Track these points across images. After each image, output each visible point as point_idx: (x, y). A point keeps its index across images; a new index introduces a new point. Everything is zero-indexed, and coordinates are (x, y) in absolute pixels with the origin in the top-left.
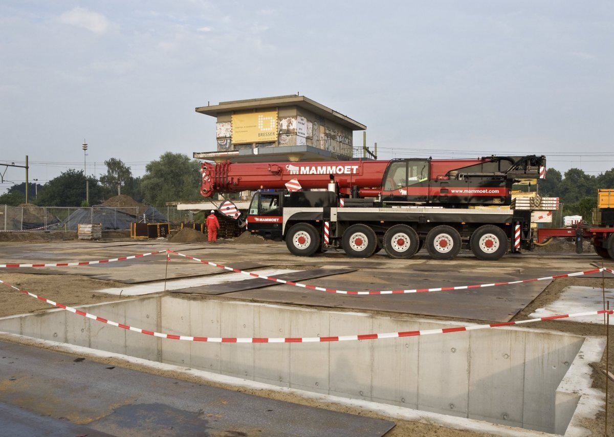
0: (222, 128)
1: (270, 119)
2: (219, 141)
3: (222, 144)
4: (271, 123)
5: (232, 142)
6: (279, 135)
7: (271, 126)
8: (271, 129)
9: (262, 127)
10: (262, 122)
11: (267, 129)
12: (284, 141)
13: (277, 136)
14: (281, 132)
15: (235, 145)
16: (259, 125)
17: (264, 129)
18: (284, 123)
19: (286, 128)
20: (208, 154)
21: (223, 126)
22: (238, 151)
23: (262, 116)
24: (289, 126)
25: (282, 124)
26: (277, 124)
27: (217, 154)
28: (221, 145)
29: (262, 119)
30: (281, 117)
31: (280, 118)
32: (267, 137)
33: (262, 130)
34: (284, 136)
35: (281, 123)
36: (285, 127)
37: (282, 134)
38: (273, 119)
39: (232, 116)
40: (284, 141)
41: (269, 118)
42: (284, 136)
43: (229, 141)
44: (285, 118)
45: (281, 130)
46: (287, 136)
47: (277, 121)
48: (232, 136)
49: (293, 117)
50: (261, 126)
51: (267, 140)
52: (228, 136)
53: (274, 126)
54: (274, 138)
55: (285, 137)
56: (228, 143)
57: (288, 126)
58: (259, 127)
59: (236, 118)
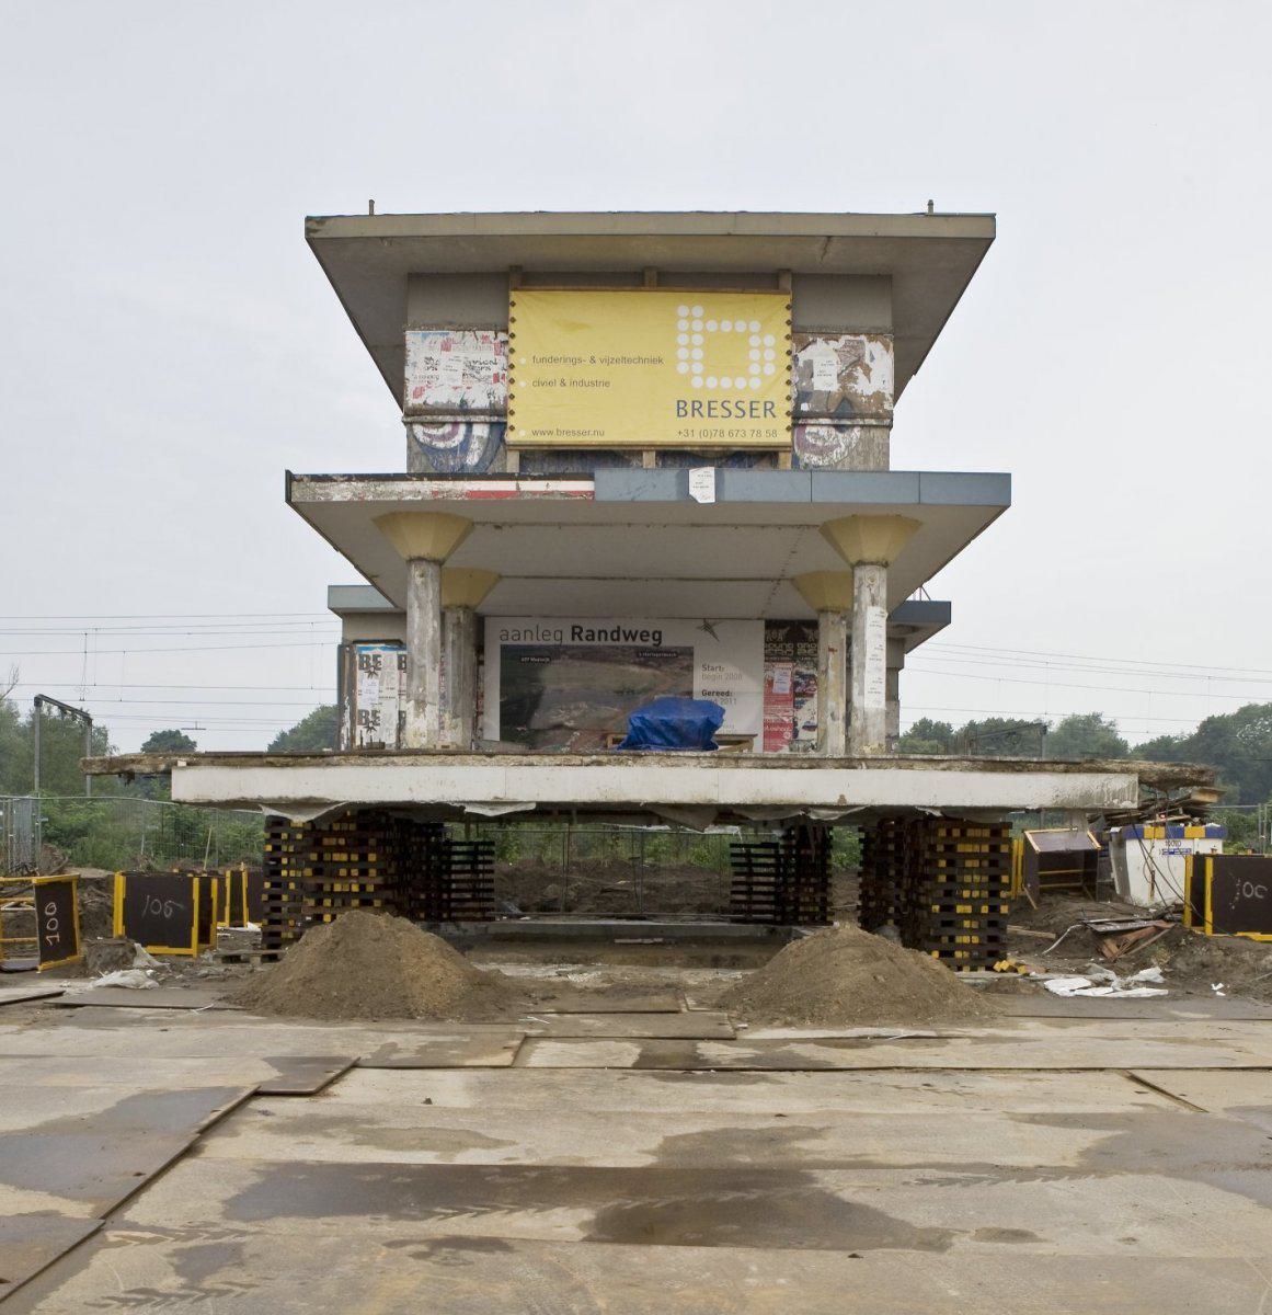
0: (442, 357)
1: (748, 334)
2: (418, 430)
3: (441, 445)
4: (754, 355)
5: (511, 437)
6: (798, 420)
7: (754, 369)
8: (755, 384)
9: (698, 368)
10: (698, 339)
11: (726, 383)
12: (821, 452)
13: (788, 421)
14: (805, 407)
16: (682, 354)
17: (712, 382)
18: (825, 363)
19: (834, 386)
20: (382, 487)
21: (446, 347)
22: (591, 477)
23: (698, 311)
24: (851, 377)
25: (809, 364)
26: (788, 360)
27: (448, 485)
28: (428, 450)
29: (698, 326)
30: (804, 330)
31: (800, 335)
32: (732, 424)
33: (697, 382)
34: (819, 431)
35: (803, 356)
36: (826, 381)
37: (809, 415)
38: (761, 334)
39: (514, 296)
40: (821, 452)
41: (741, 326)
42: (819, 431)
43: (481, 431)
44: (830, 334)
45: (803, 396)
46: (839, 428)
47: (788, 345)
48: (512, 405)
49: (873, 335)
50: (690, 361)
51: (727, 439)
52: (480, 401)
53: (770, 369)
54: (773, 430)
55: (823, 431)
56: (475, 445)
57: (846, 378)
58: (683, 368)
59: (533, 315)
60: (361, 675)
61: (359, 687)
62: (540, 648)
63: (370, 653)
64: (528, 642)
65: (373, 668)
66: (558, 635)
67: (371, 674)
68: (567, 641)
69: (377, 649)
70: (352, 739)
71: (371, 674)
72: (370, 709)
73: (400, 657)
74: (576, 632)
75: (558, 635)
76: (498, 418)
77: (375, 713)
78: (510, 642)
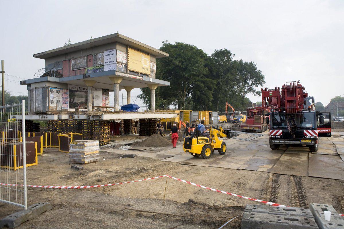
15: (131, 71)
60: (50, 93)
61: (50, 95)
63: (52, 89)
64: (73, 89)
65: (52, 92)
67: (52, 93)
68: (78, 90)
69: (53, 89)
70: (49, 105)
71: (52, 93)
72: (52, 99)
73: (57, 90)
74: (80, 88)
76: (127, 66)
77: (53, 100)
78: (70, 89)
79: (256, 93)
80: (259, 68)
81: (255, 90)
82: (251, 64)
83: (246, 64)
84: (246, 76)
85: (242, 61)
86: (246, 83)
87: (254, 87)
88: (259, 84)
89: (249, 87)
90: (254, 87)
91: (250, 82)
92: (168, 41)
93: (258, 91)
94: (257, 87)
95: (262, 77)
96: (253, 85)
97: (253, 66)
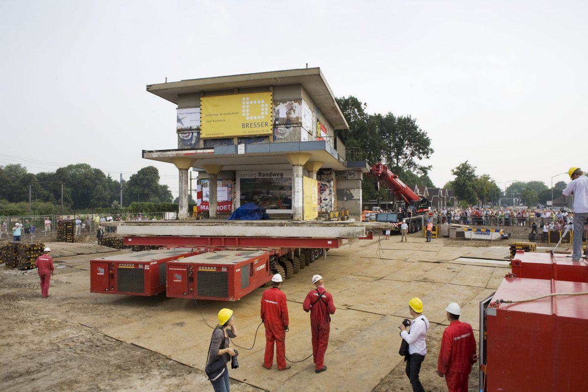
62: (251, 179)
66: (255, 175)
75: (255, 175)
79: (420, 169)
80: (422, 126)
81: (416, 164)
82: (409, 120)
83: (400, 120)
84: (401, 141)
85: (392, 114)
86: (399, 153)
87: (415, 159)
88: (424, 154)
89: (405, 160)
90: (415, 159)
91: (407, 151)
92: (307, 64)
93: (423, 166)
94: (421, 158)
95: (426, 143)
96: (413, 156)
97: (412, 123)
